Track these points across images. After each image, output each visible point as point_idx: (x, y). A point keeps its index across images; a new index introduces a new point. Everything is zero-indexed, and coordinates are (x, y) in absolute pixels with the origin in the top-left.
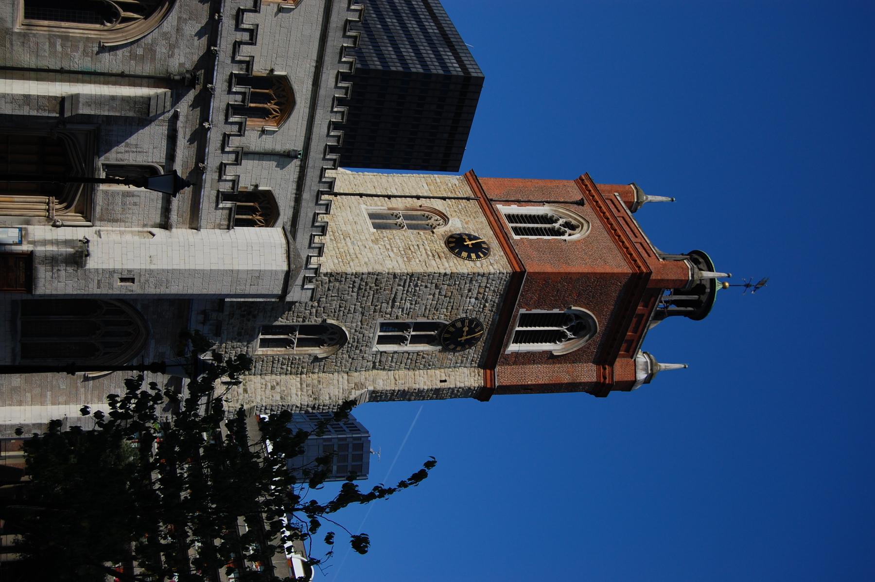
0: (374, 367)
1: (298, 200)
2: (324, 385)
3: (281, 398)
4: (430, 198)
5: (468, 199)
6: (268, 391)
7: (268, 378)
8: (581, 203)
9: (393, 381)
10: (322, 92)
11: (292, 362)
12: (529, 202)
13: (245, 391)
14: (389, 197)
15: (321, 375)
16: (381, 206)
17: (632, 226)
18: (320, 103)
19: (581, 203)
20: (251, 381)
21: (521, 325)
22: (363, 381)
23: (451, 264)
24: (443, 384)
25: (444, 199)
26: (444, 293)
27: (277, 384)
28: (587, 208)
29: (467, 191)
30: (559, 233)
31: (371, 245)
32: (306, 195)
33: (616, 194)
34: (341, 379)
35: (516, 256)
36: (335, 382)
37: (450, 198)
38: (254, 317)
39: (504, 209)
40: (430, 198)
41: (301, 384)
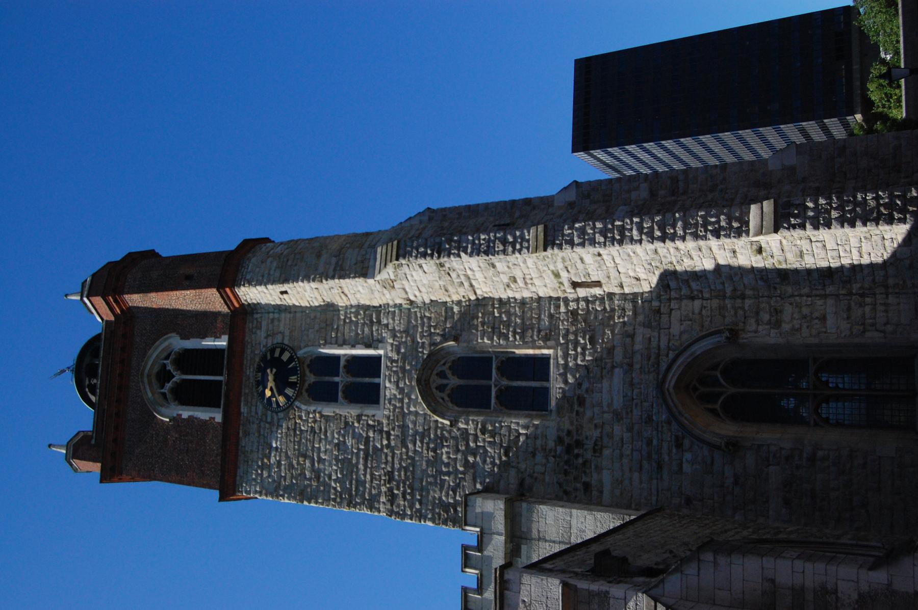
0: (378, 309)
2: (437, 285)
3: (494, 266)
6: (519, 275)
7: (527, 294)
9: (346, 291)
11: (495, 329)
13: (557, 275)
15: (448, 300)
20: (554, 289)
21: (221, 382)
22: (385, 291)
24: (283, 289)
26: (308, 464)
27: (508, 286)
34: (417, 293)
36: (423, 289)
38: (560, 440)
41: (471, 285)
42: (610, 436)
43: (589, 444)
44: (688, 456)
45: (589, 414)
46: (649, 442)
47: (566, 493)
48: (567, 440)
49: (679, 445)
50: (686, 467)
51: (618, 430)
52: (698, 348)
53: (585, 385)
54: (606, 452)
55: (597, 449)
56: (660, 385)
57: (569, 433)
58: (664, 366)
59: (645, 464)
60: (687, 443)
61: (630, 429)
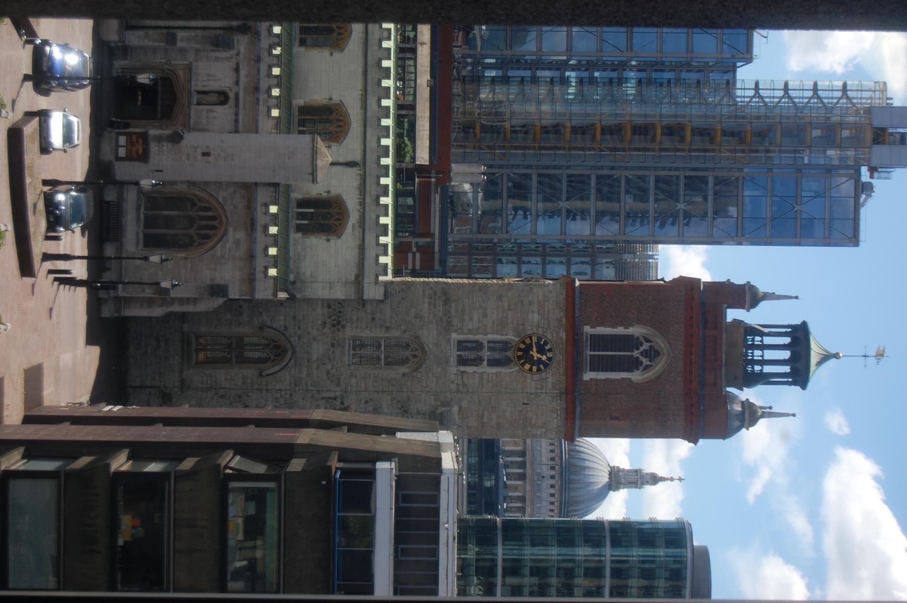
1: (363, 204)
10: (369, 114)
18: (368, 123)
32: (368, 200)
38: (343, 327)
42: (318, 330)
43: (328, 326)
44: (282, 323)
45: (329, 339)
46: (299, 328)
47: (340, 303)
48: (340, 327)
49: (286, 327)
50: (282, 318)
51: (315, 333)
52: (277, 368)
53: (331, 352)
54: (320, 322)
55: (324, 323)
56: (294, 352)
57: (339, 330)
58: (293, 361)
59: (301, 318)
60: (283, 328)
61: (309, 333)
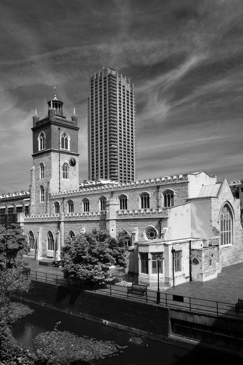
4: (60, 164)
5: (59, 155)
8: (59, 129)
12: (59, 141)
14: (60, 172)
16: (62, 175)
17: (64, 120)
19: (59, 129)
23: (77, 167)
25: (59, 160)
28: (61, 128)
29: (57, 154)
30: (67, 140)
31: (73, 181)
33: (55, 116)
35: (76, 154)
37: (59, 159)
39: (61, 148)
40: (60, 164)
